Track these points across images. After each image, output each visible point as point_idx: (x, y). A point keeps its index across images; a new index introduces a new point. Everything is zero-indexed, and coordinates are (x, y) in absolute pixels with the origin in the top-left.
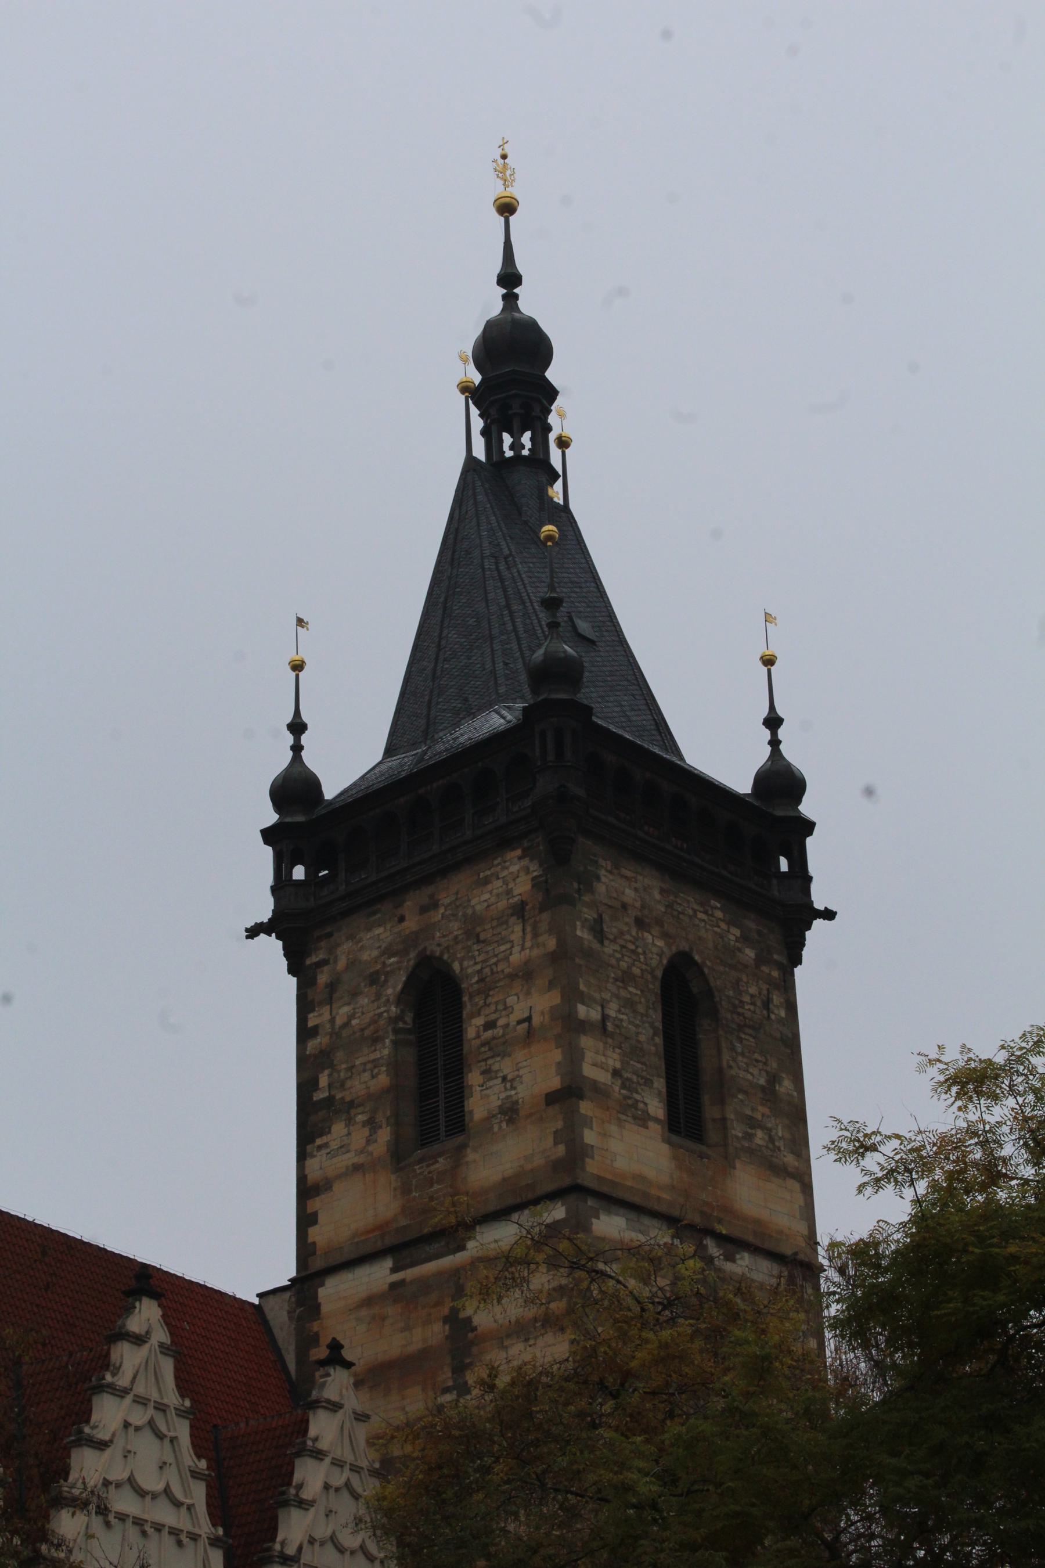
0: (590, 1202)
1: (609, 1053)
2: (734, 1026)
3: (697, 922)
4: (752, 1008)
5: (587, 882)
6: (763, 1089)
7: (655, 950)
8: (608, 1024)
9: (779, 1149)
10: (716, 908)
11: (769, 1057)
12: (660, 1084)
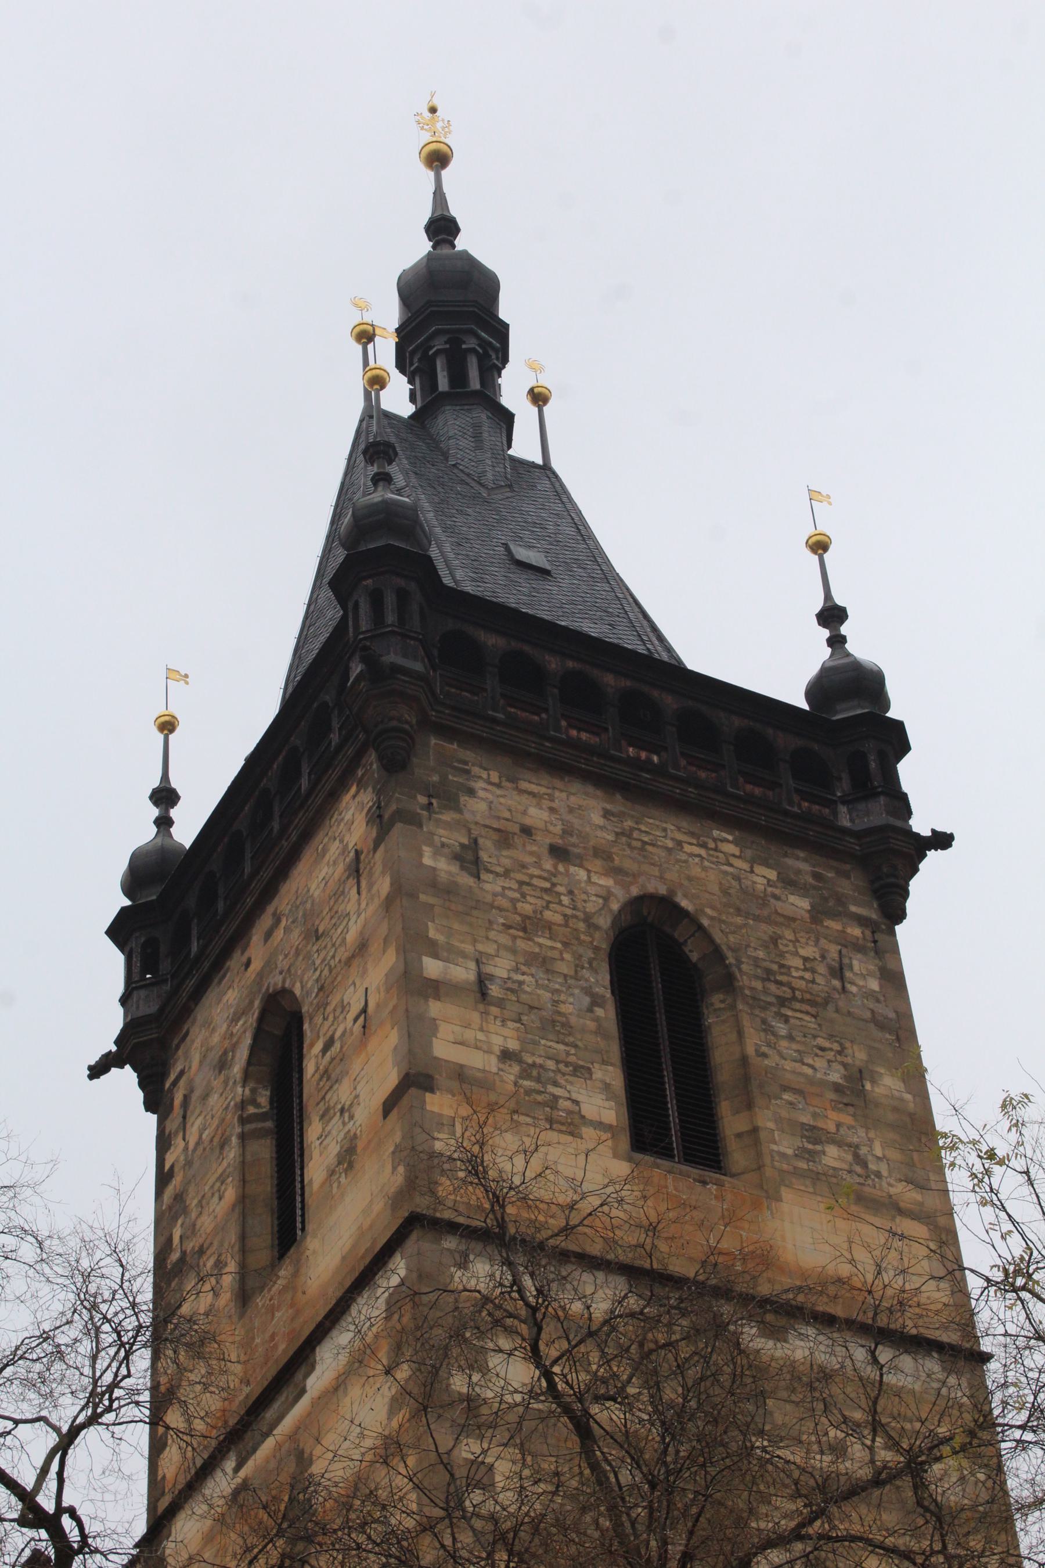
0: (450, 1243)
1: (494, 1026)
3: (684, 857)
4: (808, 975)
6: (837, 1088)
8: (493, 987)
9: (878, 1175)
10: (728, 841)
11: (848, 1044)
12: (613, 1075)
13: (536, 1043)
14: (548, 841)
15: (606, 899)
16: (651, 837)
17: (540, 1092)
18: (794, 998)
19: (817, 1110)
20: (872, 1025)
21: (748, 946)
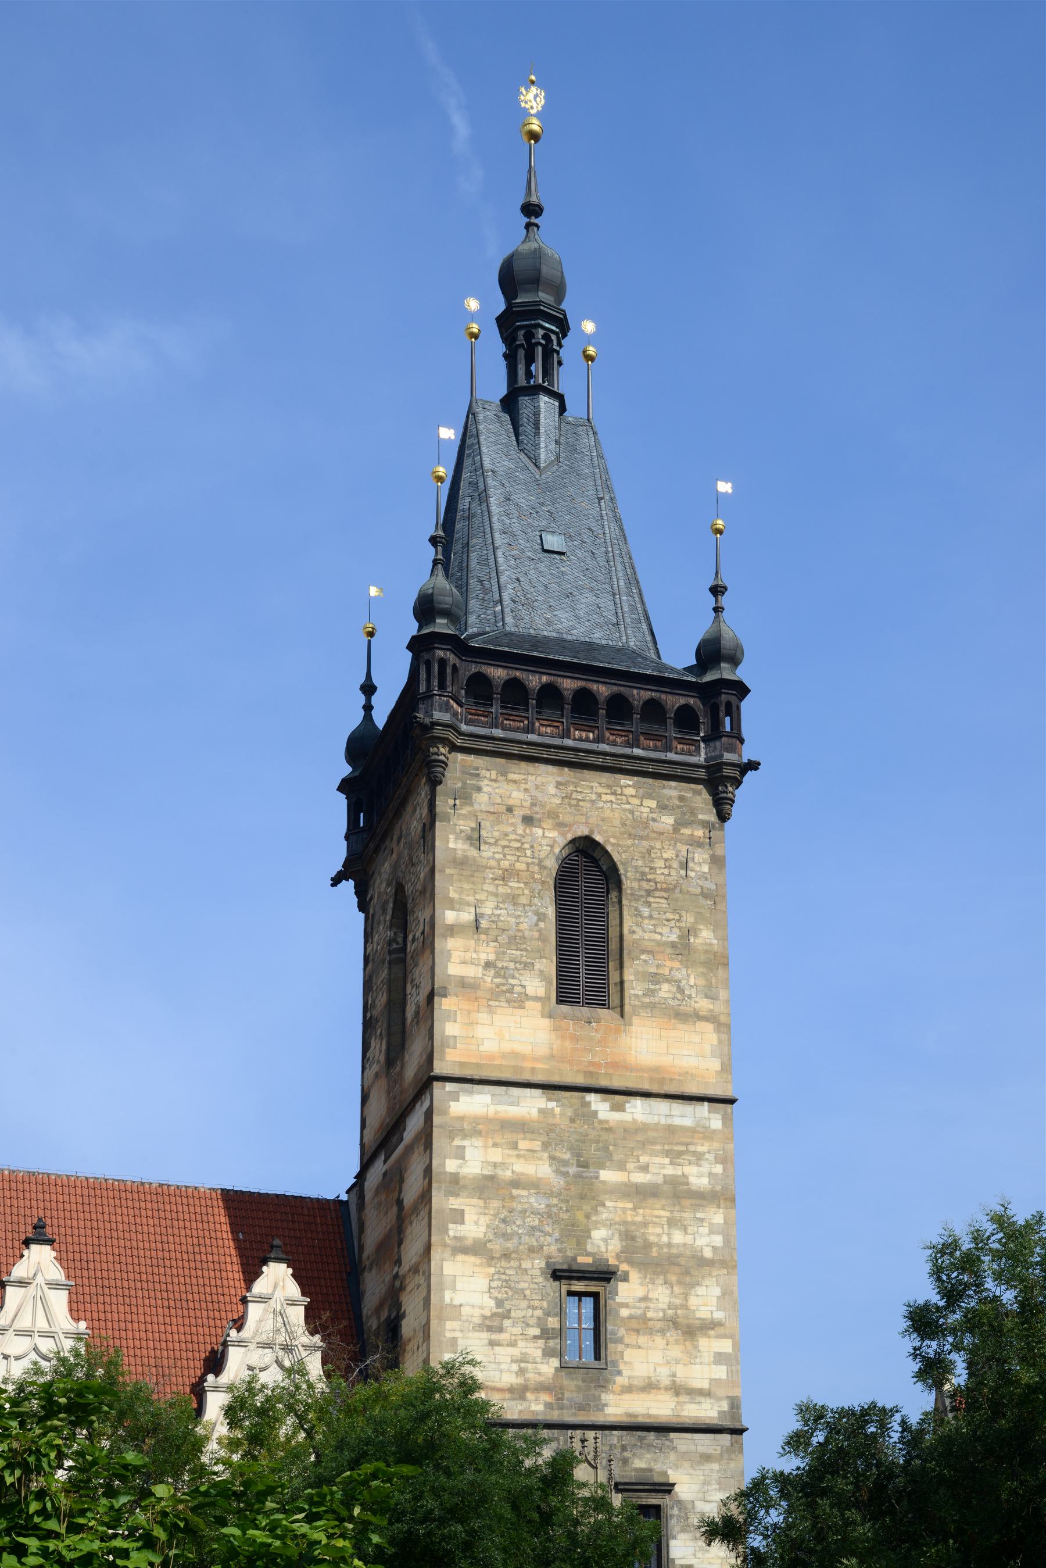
1: (483, 947)
2: (643, 893)
3: (601, 804)
4: (666, 871)
6: (673, 945)
7: (544, 842)
9: (690, 997)
10: (629, 786)
13: (504, 953)
14: (522, 813)
15: (552, 847)
16: (583, 795)
17: (504, 985)
18: (656, 889)
19: (660, 962)
20: (700, 897)
21: (633, 859)
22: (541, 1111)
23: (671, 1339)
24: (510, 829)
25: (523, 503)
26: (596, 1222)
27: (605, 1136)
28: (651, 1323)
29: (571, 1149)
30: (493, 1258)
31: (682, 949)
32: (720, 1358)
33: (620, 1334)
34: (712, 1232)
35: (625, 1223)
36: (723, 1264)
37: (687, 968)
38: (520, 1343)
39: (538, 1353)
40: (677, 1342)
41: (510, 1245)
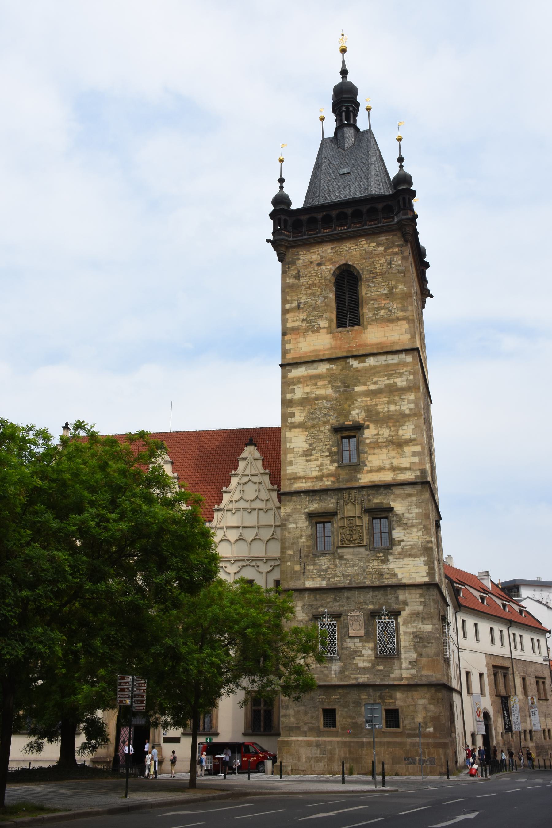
3: (351, 251)
4: (381, 268)
5: (293, 263)
6: (386, 294)
7: (326, 270)
9: (394, 313)
15: (330, 271)
18: (377, 275)
22: (327, 369)
23: (390, 449)
24: (312, 269)
25: (336, 163)
26: (354, 408)
27: (356, 374)
28: (380, 444)
29: (341, 381)
30: (307, 428)
31: (390, 295)
32: (414, 454)
33: (366, 450)
34: (408, 403)
35: (367, 406)
36: (415, 415)
37: (393, 302)
38: (320, 459)
39: (328, 462)
40: (393, 450)
41: (315, 422)
